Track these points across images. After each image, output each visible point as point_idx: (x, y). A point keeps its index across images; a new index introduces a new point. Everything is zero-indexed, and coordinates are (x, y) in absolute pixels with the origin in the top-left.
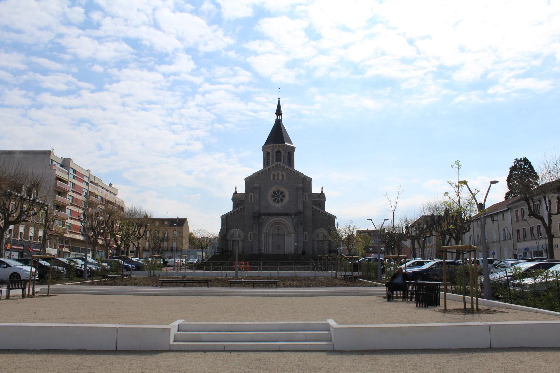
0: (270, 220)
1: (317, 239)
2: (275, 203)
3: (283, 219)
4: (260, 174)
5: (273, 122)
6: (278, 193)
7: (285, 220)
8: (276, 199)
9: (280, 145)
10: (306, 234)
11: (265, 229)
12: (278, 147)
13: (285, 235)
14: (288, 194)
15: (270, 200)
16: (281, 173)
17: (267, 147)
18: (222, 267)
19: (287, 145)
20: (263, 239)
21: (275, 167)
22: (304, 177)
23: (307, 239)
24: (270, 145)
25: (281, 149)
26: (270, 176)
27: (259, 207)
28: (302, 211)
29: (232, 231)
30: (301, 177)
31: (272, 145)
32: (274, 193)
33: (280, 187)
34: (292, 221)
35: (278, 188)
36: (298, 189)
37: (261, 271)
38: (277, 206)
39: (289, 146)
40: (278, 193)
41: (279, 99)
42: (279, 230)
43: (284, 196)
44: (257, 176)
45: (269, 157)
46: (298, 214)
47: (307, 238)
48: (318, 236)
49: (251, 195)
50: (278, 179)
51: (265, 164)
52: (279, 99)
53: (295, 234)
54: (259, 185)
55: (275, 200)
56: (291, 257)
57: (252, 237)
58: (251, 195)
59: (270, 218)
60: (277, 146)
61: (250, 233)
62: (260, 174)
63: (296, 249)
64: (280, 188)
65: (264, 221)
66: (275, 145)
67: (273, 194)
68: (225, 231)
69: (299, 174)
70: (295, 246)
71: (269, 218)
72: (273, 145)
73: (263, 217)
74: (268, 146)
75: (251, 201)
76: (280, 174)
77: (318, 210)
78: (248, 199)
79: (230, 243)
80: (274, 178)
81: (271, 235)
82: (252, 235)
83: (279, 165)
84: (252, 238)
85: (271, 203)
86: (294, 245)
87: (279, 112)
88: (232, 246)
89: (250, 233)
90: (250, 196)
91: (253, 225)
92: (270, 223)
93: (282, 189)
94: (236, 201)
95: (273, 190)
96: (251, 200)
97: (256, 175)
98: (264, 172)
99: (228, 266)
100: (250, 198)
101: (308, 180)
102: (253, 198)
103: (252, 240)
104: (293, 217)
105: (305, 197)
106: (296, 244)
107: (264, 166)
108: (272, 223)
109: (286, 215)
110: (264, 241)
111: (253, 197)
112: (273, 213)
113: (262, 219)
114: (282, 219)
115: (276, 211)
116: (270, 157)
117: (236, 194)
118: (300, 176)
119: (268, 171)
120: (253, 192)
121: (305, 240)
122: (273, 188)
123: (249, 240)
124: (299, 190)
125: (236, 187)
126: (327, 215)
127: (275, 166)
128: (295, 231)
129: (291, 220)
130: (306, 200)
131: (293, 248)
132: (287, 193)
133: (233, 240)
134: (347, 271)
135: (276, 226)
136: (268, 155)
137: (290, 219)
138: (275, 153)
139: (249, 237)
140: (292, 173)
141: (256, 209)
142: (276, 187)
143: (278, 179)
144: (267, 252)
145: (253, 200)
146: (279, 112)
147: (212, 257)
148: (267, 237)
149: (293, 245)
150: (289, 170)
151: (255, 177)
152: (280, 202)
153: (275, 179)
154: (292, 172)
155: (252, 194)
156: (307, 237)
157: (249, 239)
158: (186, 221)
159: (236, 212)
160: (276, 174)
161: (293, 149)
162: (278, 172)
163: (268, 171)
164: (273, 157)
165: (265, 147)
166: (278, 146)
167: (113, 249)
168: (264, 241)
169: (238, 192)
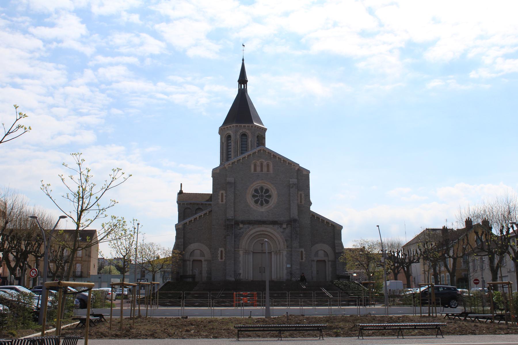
0: (250, 230)
1: (316, 259)
2: (257, 205)
3: (269, 229)
4: (236, 163)
5: (234, 93)
6: (262, 191)
7: (272, 231)
8: (258, 200)
9: (247, 125)
10: (302, 252)
11: (244, 243)
12: (244, 128)
13: (272, 253)
14: (276, 193)
15: (250, 201)
16: (266, 162)
17: (227, 128)
18: (213, 301)
19: (256, 126)
20: (241, 259)
21: (257, 154)
22: (298, 169)
23: (304, 259)
24: (231, 126)
25: (247, 131)
26: (250, 166)
27: (235, 211)
28: (297, 218)
29: (192, 247)
30: (295, 168)
31: (234, 125)
32: (256, 191)
33: (265, 183)
34: (283, 232)
35: (263, 184)
36: (291, 186)
37: (213, 307)
38: (261, 210)
39: (258, 127)
40: (262, 191)
41: (243, 60)
42: (263, 245)
43: (270, 196)
45: (229, 142)
46: (291, 222)
47: (304, 257)
48: (317, 254)
49: (222, 194)
50: (262, 171)
51: (224, 151)
52: (243, 60)
54: (233, 179)
55: (256, 202)
56: (284, 285)
57: (224, 255)
58: (222, 194)
59: (251, 227)
60: (241, 126)
61: (220, 249)
62: (236, 163)
63: (291, 273)
64: (265, 184)
65: (243, 232)
66: (239, 125)
67: (253, 192)
68: (183, 246)
69: (291, 164)
70: (287, 268)
71: (249, 228)
72: (237, 125)
73: (241, 226)
74: (228, 126)
75: (222, 203)
76: (265, 163)
77: (317, 217)
78: (219, 199)
79: (189, 264)
80: (255, 170)
81: (252, 252)
82: (224, 252)
83: (263, 150)
84: (223, 257)
85: (252, 206)
86: (287, 267)
87: (243, 80)
88: (191, 268)
89: (220, 249)
90: (220, 195)
91: (225, 238)
92: (251, 235)
93: (268, 185)
94: (183, 204)
95: (255, 186)
96: (222, 201)
97: (230, 164)
98: (241, 161)
99: (338, 298)
100: (220, 197)
101: (304, 173)
102: (224, 198)
103: (223, 260)
104: (284, 226)
105: (301, 197)
106: (289, 266)
108: (253, 236)
109: (274, 223)
110: (242, 262)
111: (226, 196)
112: (255, 221)
113: (240, 229)
114: (269, 229)
115: (259, 218)
116: (232, 142)
117: (182, 195)
119: (246, 158)
120: (224, 190)
121: (300, 261)
122: (254, 183)
123: (220, 260)
124: (292, 188)
125: (181, 184)
126: (330, 224)
127: (257, 151)
128: (287, 247)
129: (282, 230)
130: (301, 202)
131: (285, 272)
132: (274, 192)
133: (194, 261)
134: (417, 306)
135: (259, 239)
136: (229, 139)
139: (219, 255)
141: (230, 214)
143: (262, 171)
144: (247, 278)
145: (224, 201)
146: (243, 80)
147: (165, 285)
149: (285, 268)
150: (277, 159)
151: (229, 167)
152: (265, 204)
153: (257, 170)
154: (282, 162)
155: (224, 192)
156: (304, 256)
157: (219, 258)
158: (95, 234)
159: (198, 219)
160: (258, 163)
161: (265, 130)
162: (262, 160)
163: (246, 158)
164: (236, 142)
165: (224, 128)
166: (244, 126)
167: (33, 272)
169: (184, 192)
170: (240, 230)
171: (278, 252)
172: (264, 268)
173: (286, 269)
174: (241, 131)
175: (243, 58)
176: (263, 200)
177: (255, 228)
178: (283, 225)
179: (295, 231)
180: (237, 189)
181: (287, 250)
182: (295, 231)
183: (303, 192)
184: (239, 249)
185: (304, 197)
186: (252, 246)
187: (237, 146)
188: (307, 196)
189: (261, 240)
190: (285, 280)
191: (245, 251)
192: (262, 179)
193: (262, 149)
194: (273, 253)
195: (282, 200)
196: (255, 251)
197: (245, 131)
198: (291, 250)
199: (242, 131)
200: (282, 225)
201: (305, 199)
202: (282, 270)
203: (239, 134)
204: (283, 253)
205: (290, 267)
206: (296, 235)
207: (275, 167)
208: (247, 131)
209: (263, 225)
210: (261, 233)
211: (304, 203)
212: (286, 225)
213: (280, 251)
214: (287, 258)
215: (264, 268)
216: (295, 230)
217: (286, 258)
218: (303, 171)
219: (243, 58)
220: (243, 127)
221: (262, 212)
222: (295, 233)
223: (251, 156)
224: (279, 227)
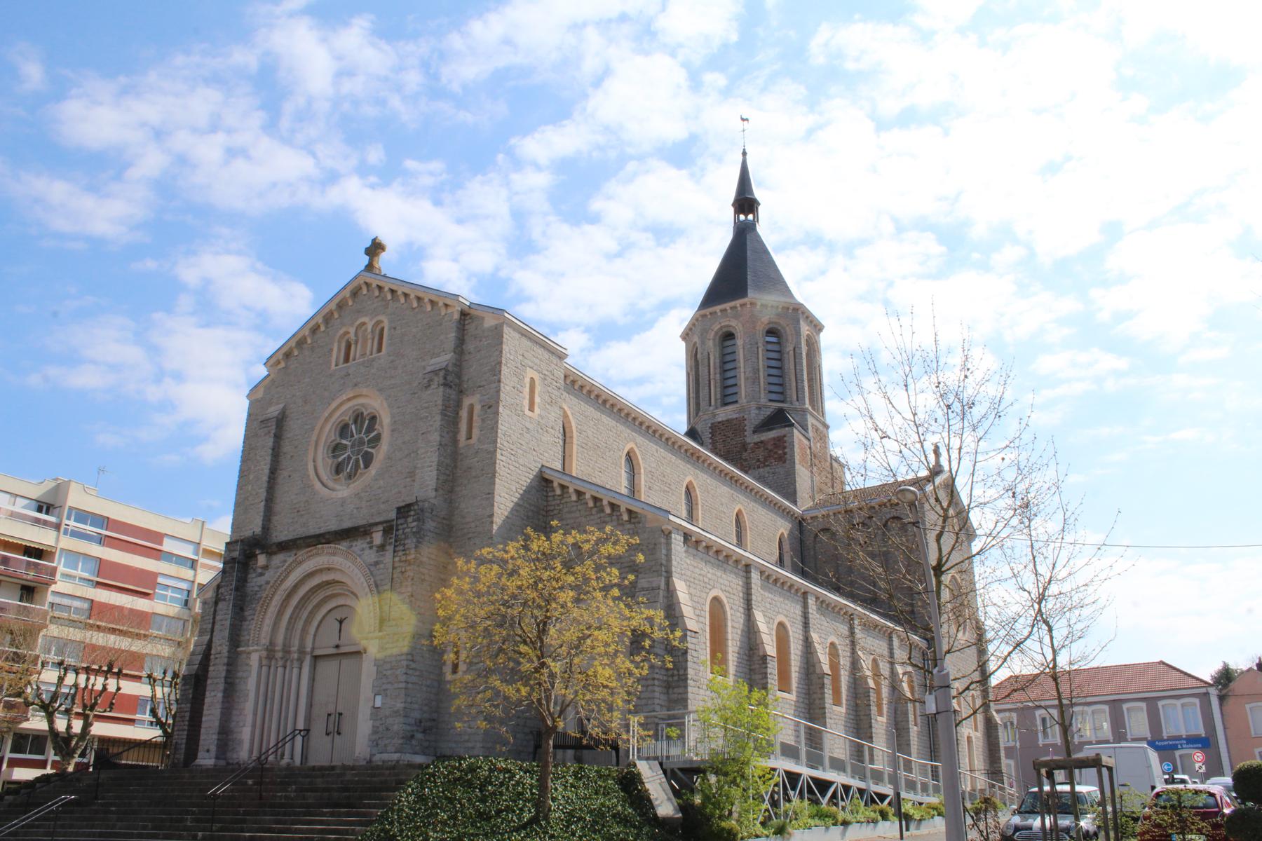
0: (288, 572)
2: (335, 480)
5: (723, 239)
9: (727, 306)
25: (733, 323)
34: (376, 563)
41: (744, 154)
42: (343, 625)
44: (283, 365)
51: (691, 395)
52: (744, 154)
60: (716, 312)
62: (296, 353)
65: (268, 583)
86: (374, 707)
97: (278, 362)
101: (489, 322)
104: (378, 538)
107: (698, 404)
113: (261, 575)
115: (333, 526)
118: (443, 312)
122: (334, 405)
129: (371, 556)
137: (367, 552)
138: (711, 343)
140: (414, 309)
142: (344, 397)
163: (322, 328)
166: (721, 311)
168: (252, 696)
170: (263, 578)
172: (340, 714)
173: (371, 714)
174: (716, 327)
175: (744, 150)
176: (354, 458)
177: (300, 563)
180: (288, 436)
181: (380, 634)
183: (478, 396)
184: (248, 646)
185: (479, 416)
187: (707, 371)
188: (490, 407)
190: (364, 763)
192: (356, 385)
193: (362, 282)
195: (404, 443)
196: (317, 652)
197: (726, 323)
199: (719, 326)
201: (483, 420)
203: (712, 335)
206: (403, 570)
207: (395, 328)
208: (731, 324)
209: (320, 546)
211: (479, 440)
212: (381, 533)
214: (378, 666)
216: (401, 548)
217: (375, 668)
218: (483, 318)
219: (744, 150)
220: (719, 314)
221: (343, 502)
222: (400, 561)
223: (336, 315)
224: (365, 546)
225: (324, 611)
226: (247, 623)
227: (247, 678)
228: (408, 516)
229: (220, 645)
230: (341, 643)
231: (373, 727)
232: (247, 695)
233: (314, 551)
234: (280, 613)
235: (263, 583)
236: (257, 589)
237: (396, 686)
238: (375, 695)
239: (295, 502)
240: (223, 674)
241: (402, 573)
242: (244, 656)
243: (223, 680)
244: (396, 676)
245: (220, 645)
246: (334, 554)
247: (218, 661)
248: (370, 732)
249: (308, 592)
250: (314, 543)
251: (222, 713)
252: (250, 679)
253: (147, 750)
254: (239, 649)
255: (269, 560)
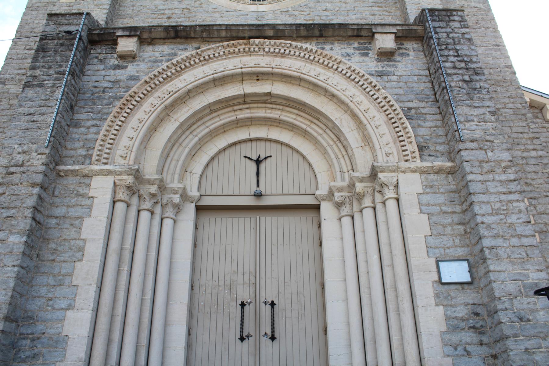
0: (180, 71)
42: (263, 166)
53: (422, 172)
65: (132, 78)
81: (190, 211)
86: (440, 282)
113: (117, 67)
128: (421, 148)
135: (242, 134)
148: (145, 215)
170: (118, 72)
171: (359, 187)
173: (437, 295)
177: (208, 60)
178: (377, 36)
179: (452, 59)
182: (452, 59)
186: (198, 167)
189: (251, 140)
191: (129, 180)
194: (326, 209)
196: (207, 202)
198: (450, 164)
200: (372, 36)
202: (406, 305)
204: (397, 186)
205: (467, 278)
206: (467, 78)
209: (257, 41)
210: (251, 88)
213: (373, 175)
215: (273, 304)
216: (451, 53)
217: (425, 217)
224: (350, 51)
225: (242, 134)
226: (82, 130)
227: (81, 218)
228: (450, 21)
229: (24, 152)
230: (263, 188)
231: (448, 318)
232: (81, 249)
233: (241, 48)
234: (153, 129)
235: (122, 78)
236: (106, 84)
237: (515, 241)
238: (437, 262)
239: (162, 7)
240: (31, 201)
241: (464, 81)
242: (71, 181)
243: (28, 213)
244: (511, 226)
245: (24, 152)
246: (283, 55)
247: (16, 178)
248: (444, 328)
249: (220, 101)
250: (247, 35)
251: (19, 278)
252: (87, 222)
253: (456, 218)
254: (62, 167)
255: (139, 49)
